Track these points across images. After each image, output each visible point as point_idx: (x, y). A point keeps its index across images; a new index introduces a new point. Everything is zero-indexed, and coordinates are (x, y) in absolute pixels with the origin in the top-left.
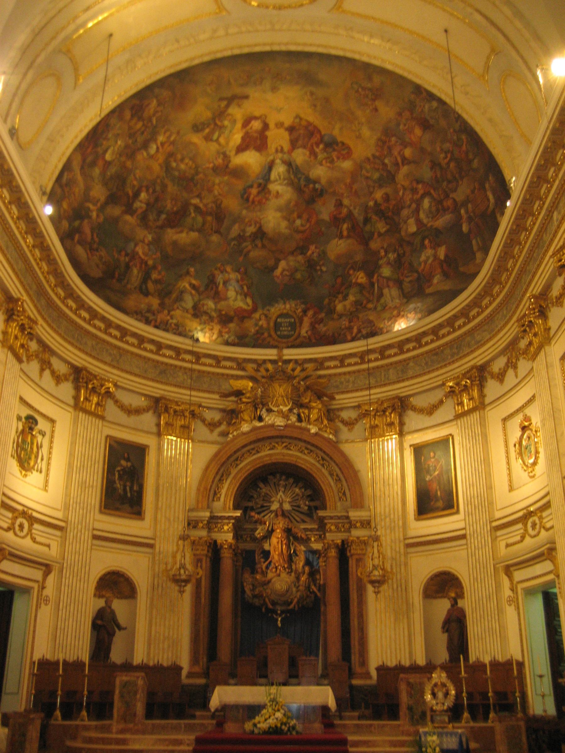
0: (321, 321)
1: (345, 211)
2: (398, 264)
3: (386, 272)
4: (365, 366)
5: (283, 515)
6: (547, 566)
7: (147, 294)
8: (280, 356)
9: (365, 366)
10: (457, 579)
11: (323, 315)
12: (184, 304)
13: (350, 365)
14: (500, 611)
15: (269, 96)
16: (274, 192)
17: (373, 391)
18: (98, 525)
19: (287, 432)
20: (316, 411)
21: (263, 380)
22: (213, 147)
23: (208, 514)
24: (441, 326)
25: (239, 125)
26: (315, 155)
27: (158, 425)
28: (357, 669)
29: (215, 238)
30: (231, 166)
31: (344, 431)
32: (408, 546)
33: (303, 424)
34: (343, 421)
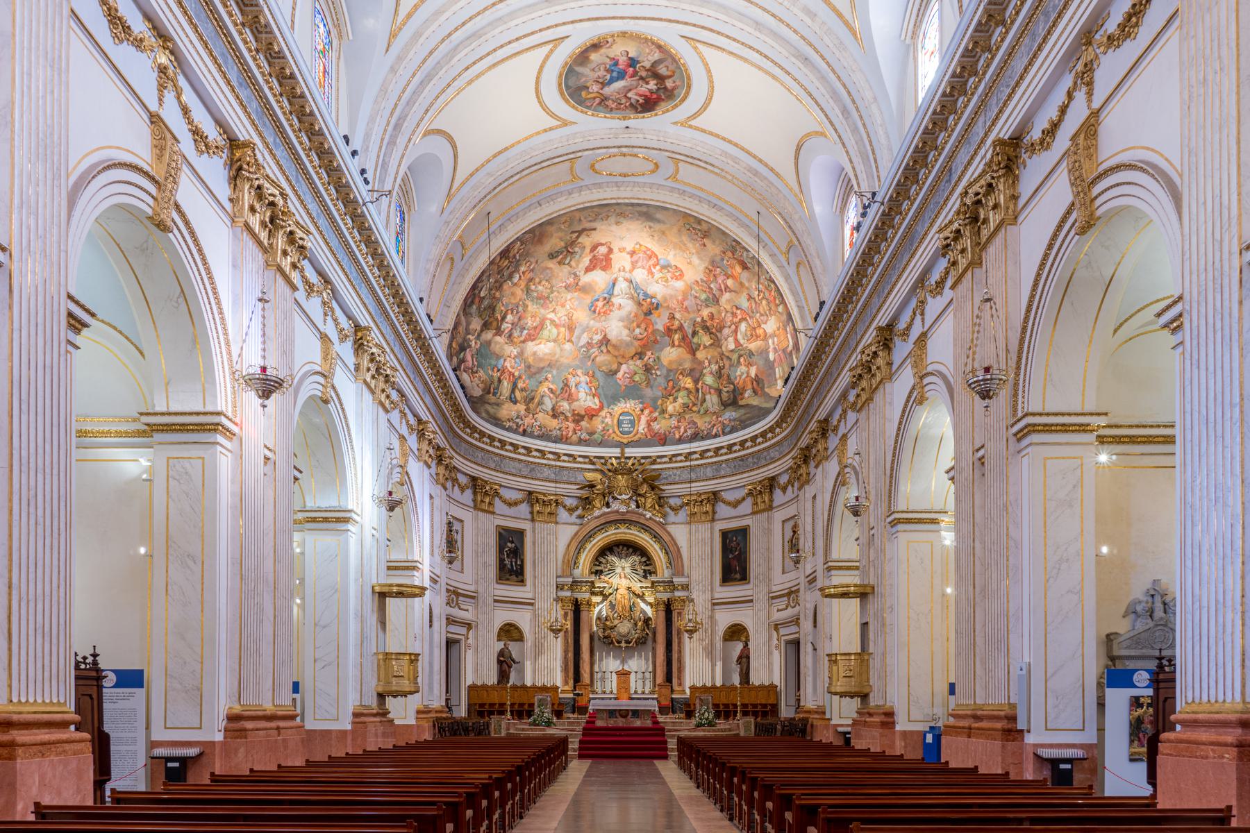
0: (655, 419)
1: (677, 323)
2: (719, 375)
3: (709, 380)
4: (688, 464)
5: (625, 577)
6: (794, 629)
7: (515, 402)
8: (623, 453)
9: (688, 464)
10: (745, 629)
11: (656, 414)
12: (544, 407)
13: (676, 462)
14: (770, 653)
15: (614, 228)
16: (616, 305)
17: (693, 485)
18: (497, 592)
19: (628, 517)
20: (650, 500)
21: (610, 474)
22: (566, 269)
23: (571, 580)
24: (746, 441)
25: (588, 250)
26: (652, 274)
27: (532, 513)
28: (676, 687)
29: (568, 346)
30: (580, 284)
31: (672, 517)
32: (714, 604)
33: (640, 510)
34: (670, 507)
